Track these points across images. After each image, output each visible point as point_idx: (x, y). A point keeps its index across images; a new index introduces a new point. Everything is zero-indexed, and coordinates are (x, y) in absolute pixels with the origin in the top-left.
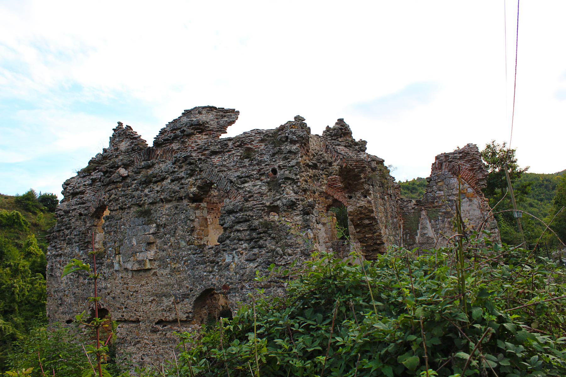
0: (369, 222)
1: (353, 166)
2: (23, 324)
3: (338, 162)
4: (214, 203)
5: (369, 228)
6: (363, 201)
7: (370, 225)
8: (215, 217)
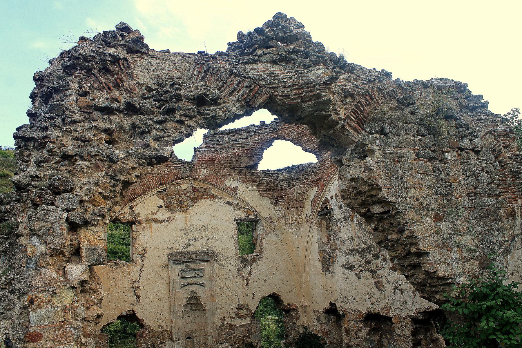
0: (382, 210)
1: (291, 97)
2: (261, 311)
3: (239, 94)
4: (282, 190)
5: (388, 221)
6: (356, 167)
7: (385, 216)
8: (288, 208)
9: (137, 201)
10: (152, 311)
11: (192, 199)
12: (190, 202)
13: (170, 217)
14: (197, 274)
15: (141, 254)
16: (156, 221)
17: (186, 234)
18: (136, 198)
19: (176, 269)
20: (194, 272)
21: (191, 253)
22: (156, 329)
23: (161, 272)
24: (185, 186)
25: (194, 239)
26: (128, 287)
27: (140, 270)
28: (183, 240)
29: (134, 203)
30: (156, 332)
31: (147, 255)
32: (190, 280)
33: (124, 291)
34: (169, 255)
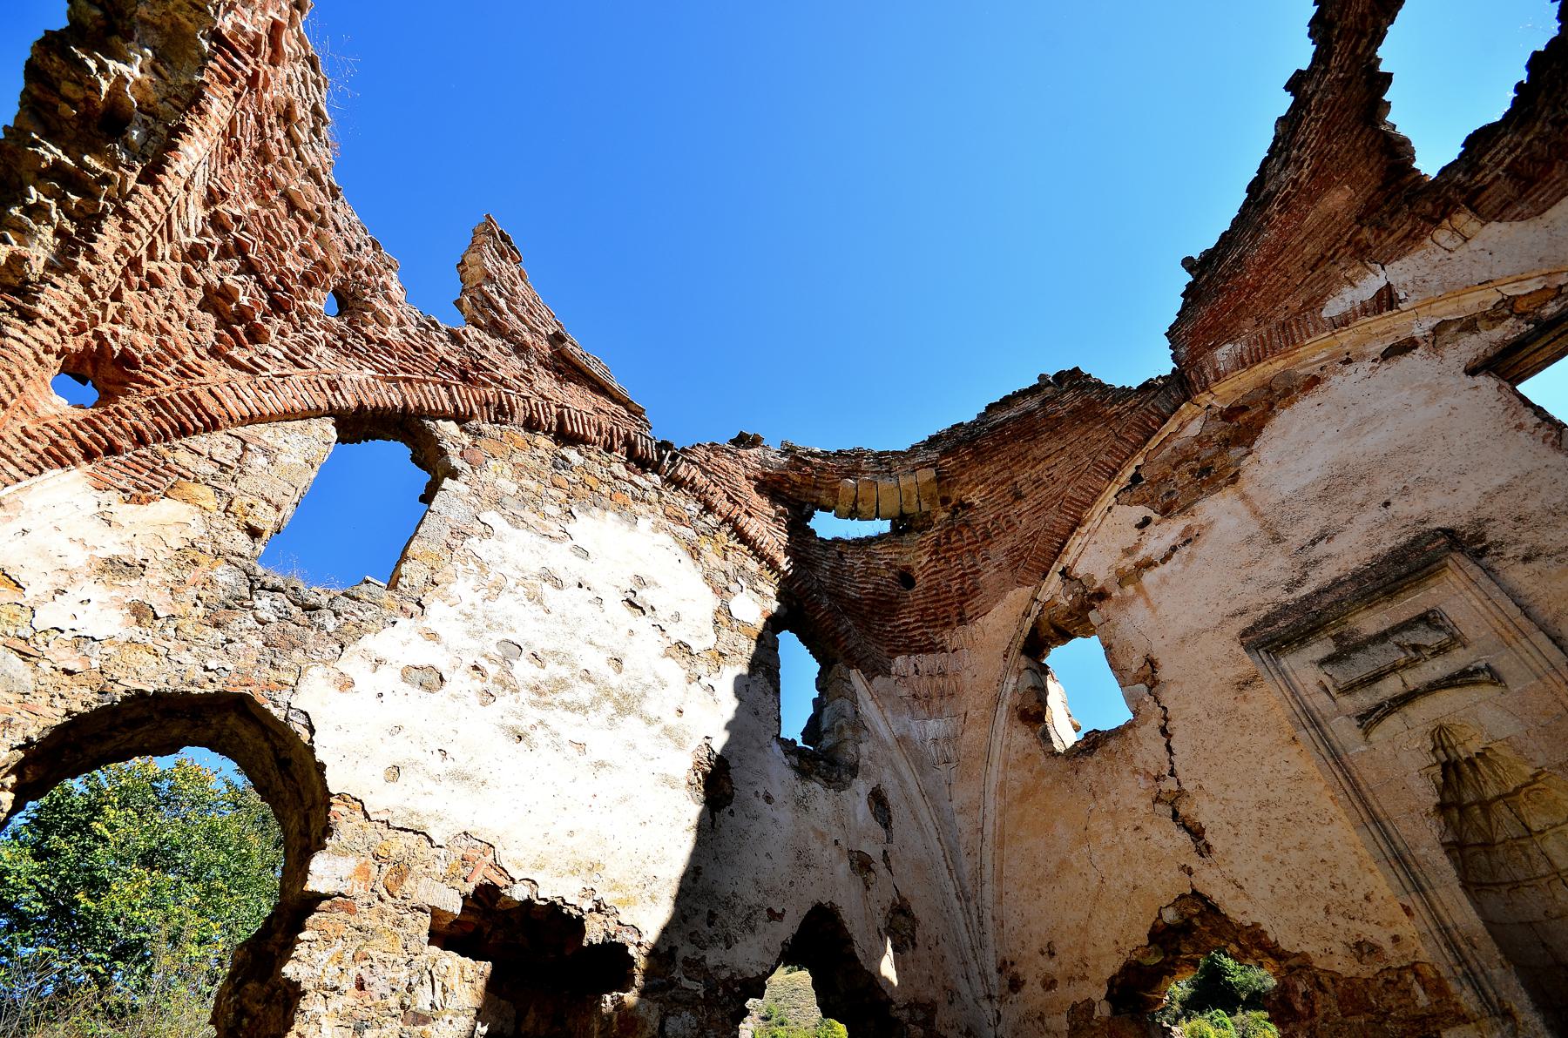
9: (1072, 550)
10: (1283, 878)
11: (1236, 437)
12: (1236, 452)
13: (1189, 528)
14: (1416, 648)
15: (1145, 679)
16: (1148, 564)
17: (1277, 539)
18: (1063, 545)
19: (1304, 666)
20: (1390, 645)
21: (1337, 583)
22: (1343, 965)
23: (1244, 707)
24: (1194, 429)
25: (1324, 536)
26: (1143, 805)
27: (1164, 731)
28: (1276, 564)
29: (1067, 560)
30: (1349, 980)
31: (1163, 675)
32: (1391, 686)
33: (1138, 823)
34: (1244, 634)
